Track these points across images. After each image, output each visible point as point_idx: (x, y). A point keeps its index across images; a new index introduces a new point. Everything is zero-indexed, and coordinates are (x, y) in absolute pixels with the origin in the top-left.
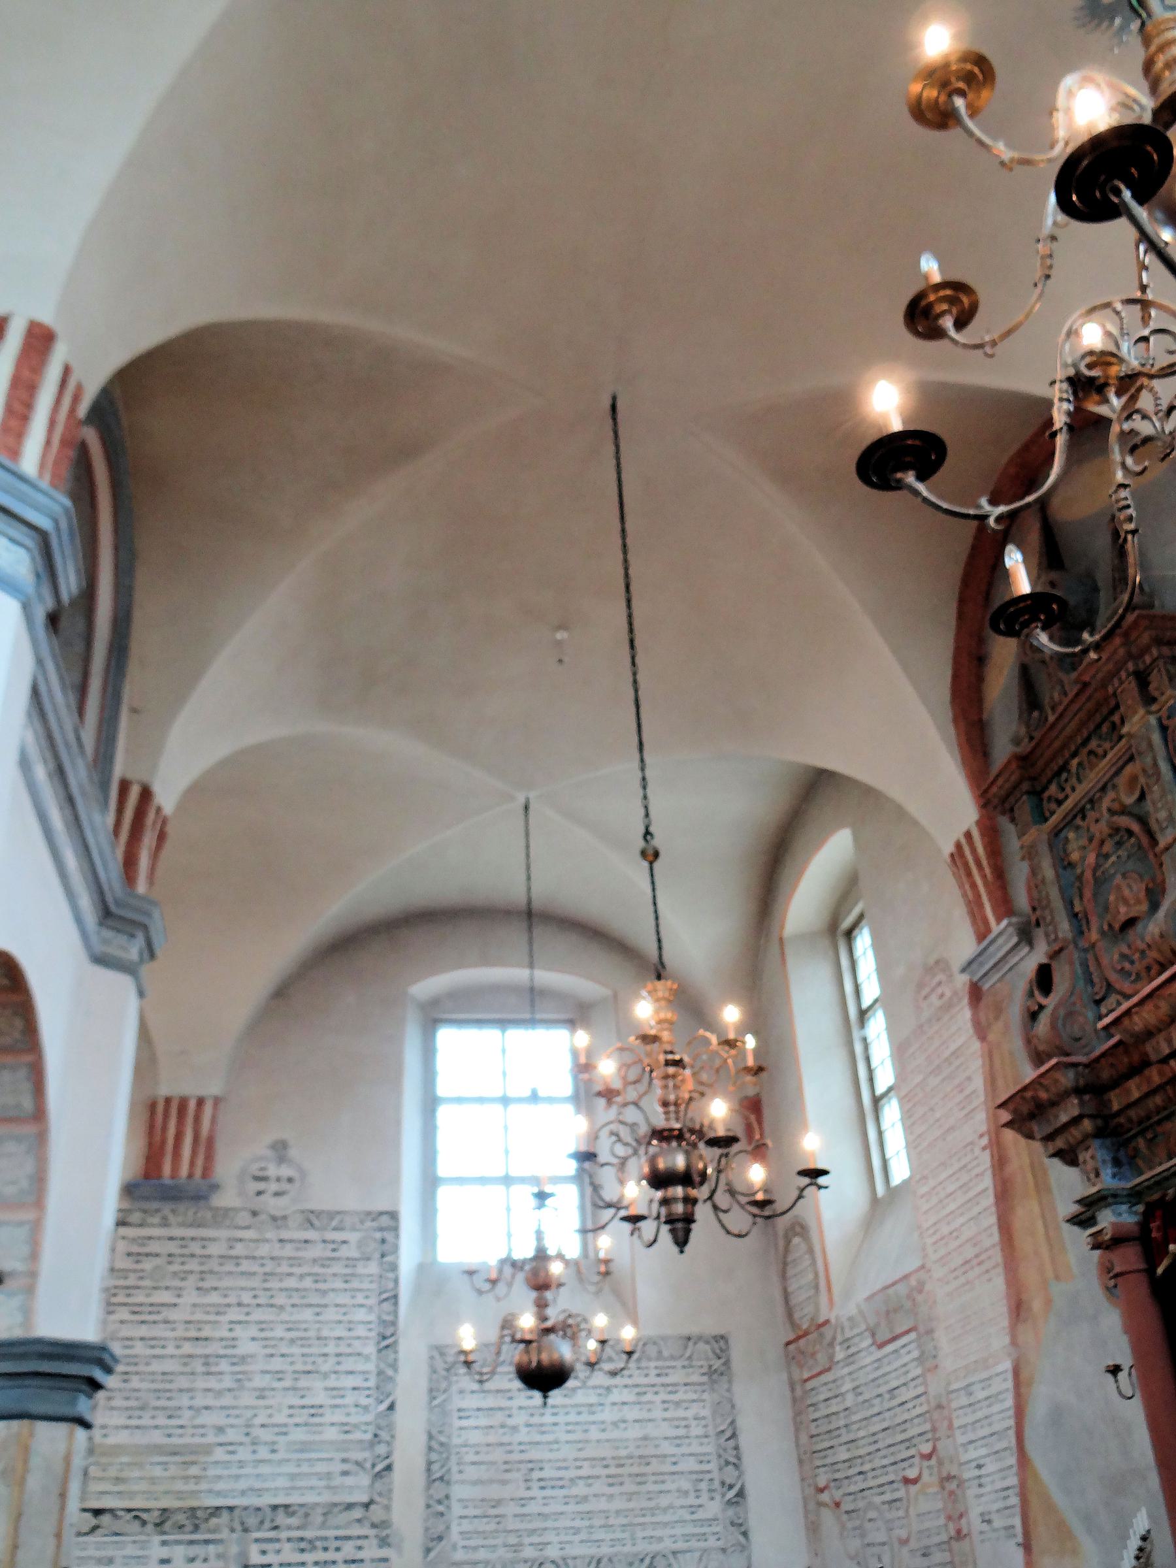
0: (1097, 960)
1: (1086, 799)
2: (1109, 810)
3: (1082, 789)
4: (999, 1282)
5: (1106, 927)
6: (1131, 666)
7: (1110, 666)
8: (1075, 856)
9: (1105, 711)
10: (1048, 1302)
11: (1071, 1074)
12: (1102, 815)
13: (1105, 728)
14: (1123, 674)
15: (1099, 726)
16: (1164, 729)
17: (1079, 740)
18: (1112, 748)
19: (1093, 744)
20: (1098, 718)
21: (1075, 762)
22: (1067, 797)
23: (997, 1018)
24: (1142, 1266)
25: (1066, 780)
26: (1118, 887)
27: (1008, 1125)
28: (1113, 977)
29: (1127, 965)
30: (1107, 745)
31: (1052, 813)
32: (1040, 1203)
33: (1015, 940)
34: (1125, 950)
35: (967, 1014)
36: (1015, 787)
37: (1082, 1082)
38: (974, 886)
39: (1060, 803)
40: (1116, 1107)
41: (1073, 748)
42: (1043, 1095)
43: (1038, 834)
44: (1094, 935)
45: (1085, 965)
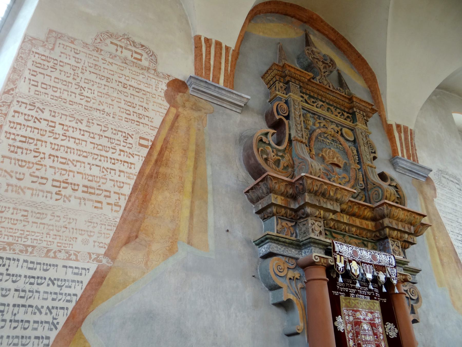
1: (324, 116)
3: (319, 110)
4: (115, 216)
7: (363, 108)
9: (342, 108)
10: (172, 251)
15: (337, 108)
17: (327, 101)
21: (321, 103)
22: (313, 106)
23: (192, 109)
32: (192, 202)
33: (243, 105)
35: (165, 88)
41: (324, 100)
42: (332, 194)
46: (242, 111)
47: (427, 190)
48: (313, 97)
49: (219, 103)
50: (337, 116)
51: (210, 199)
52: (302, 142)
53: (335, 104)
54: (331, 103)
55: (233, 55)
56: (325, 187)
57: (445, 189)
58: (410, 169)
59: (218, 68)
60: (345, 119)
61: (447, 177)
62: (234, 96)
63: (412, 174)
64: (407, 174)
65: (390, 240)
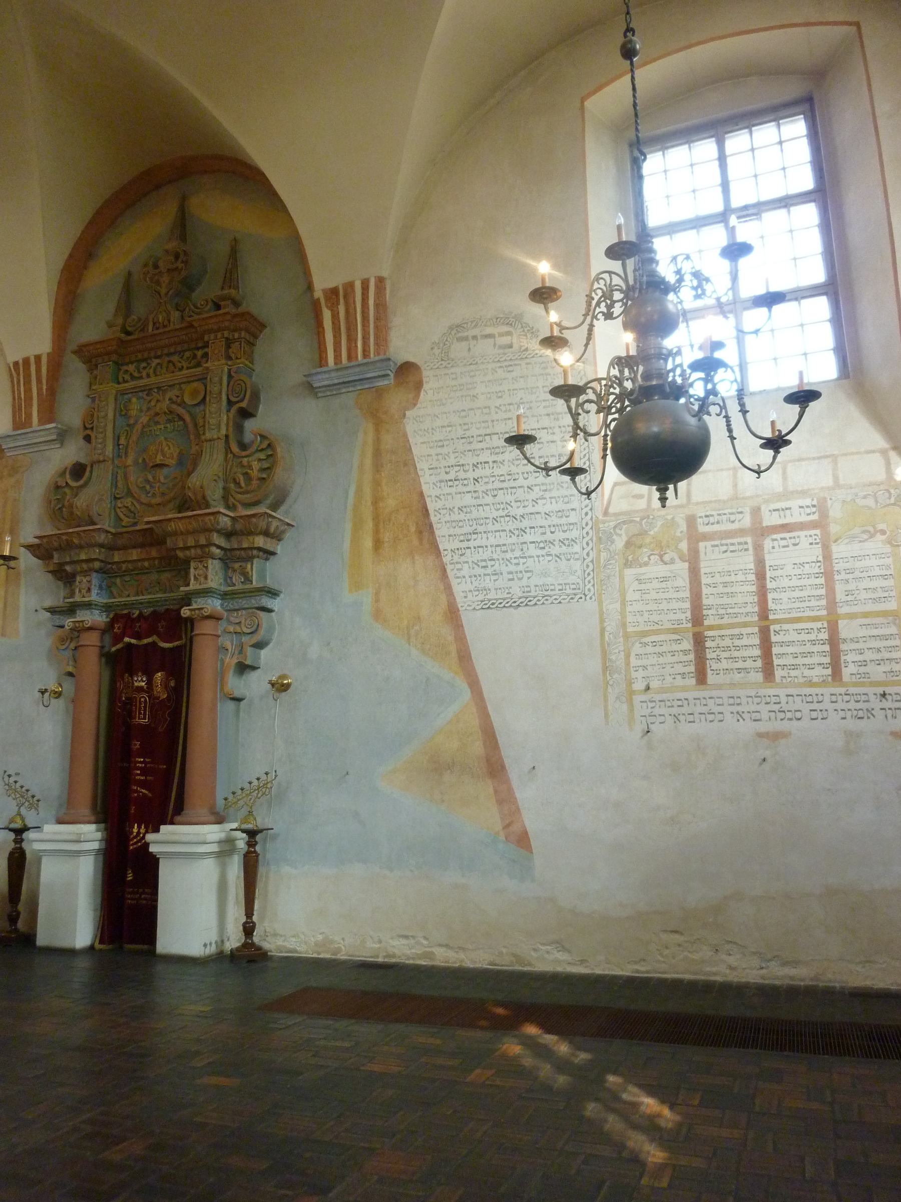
0: (125, 475)
2: (170, 399)
3: (153, 380)
5: (140, 461)
6: (226, 334)
7: (215, 327)
8: (133, 413)
11: (103, 536)
12: (164, 399)
13: (187, 354)
14: (219, 335)
15: (184, 351)
16: (230, 376)
17: (166, 351)
18: (188, 368)
19: (175, 358)
20: (186, 346)
22: (141, 378)
23: (10, 475)
24: (99, 644)
25: (144, 368)
26: (160, 443)
27: (29, 547)
28: (134, 489)
29: (148, 487)
30: (185, 365)
31: (125, 382)
33: (54, 437)
34: (150, 478)
36: (108, 354)
37: (106, 542)
38: (28, 390)
39: (133, 378)
40: (116, 559)
41: (159, 353)
42: (76, 541)
43: (111, 389)
44: (129, 462)
45: (115, 476)
46: (62, 444)
47: (395, 400)
48: (144, 360)
49: (36, 449)
50: (181, 369)
51: (23, 582)
52: (99, 462)
53: (179, 348)
54: (172, 350)
55: (48, 362)
56: (64, 537)
57: (453, 370)
58: (341, 381)
59: (29, 399)
60: (198, 365)
61: (471, 333)
62: (42, 433)
63: (354, 386)
64: (344, 390)
65: (193, 564)
